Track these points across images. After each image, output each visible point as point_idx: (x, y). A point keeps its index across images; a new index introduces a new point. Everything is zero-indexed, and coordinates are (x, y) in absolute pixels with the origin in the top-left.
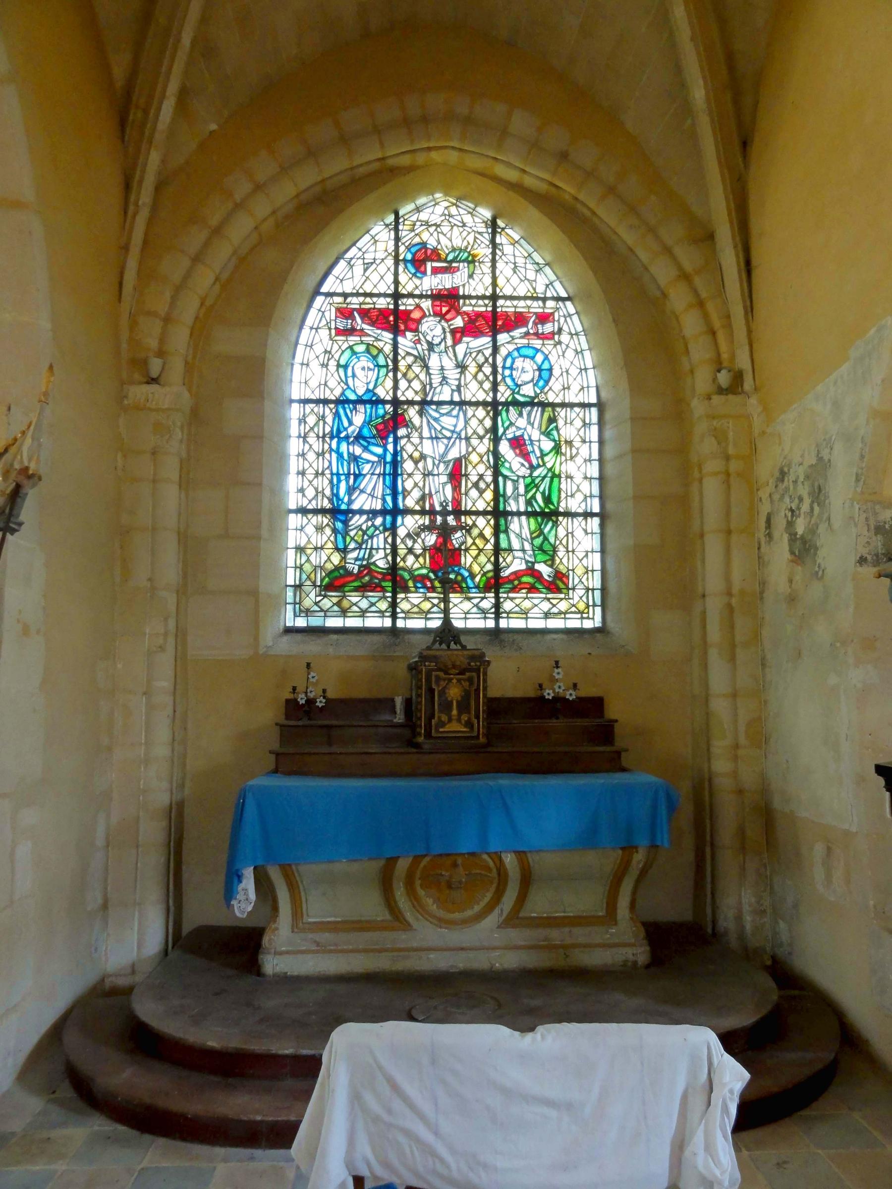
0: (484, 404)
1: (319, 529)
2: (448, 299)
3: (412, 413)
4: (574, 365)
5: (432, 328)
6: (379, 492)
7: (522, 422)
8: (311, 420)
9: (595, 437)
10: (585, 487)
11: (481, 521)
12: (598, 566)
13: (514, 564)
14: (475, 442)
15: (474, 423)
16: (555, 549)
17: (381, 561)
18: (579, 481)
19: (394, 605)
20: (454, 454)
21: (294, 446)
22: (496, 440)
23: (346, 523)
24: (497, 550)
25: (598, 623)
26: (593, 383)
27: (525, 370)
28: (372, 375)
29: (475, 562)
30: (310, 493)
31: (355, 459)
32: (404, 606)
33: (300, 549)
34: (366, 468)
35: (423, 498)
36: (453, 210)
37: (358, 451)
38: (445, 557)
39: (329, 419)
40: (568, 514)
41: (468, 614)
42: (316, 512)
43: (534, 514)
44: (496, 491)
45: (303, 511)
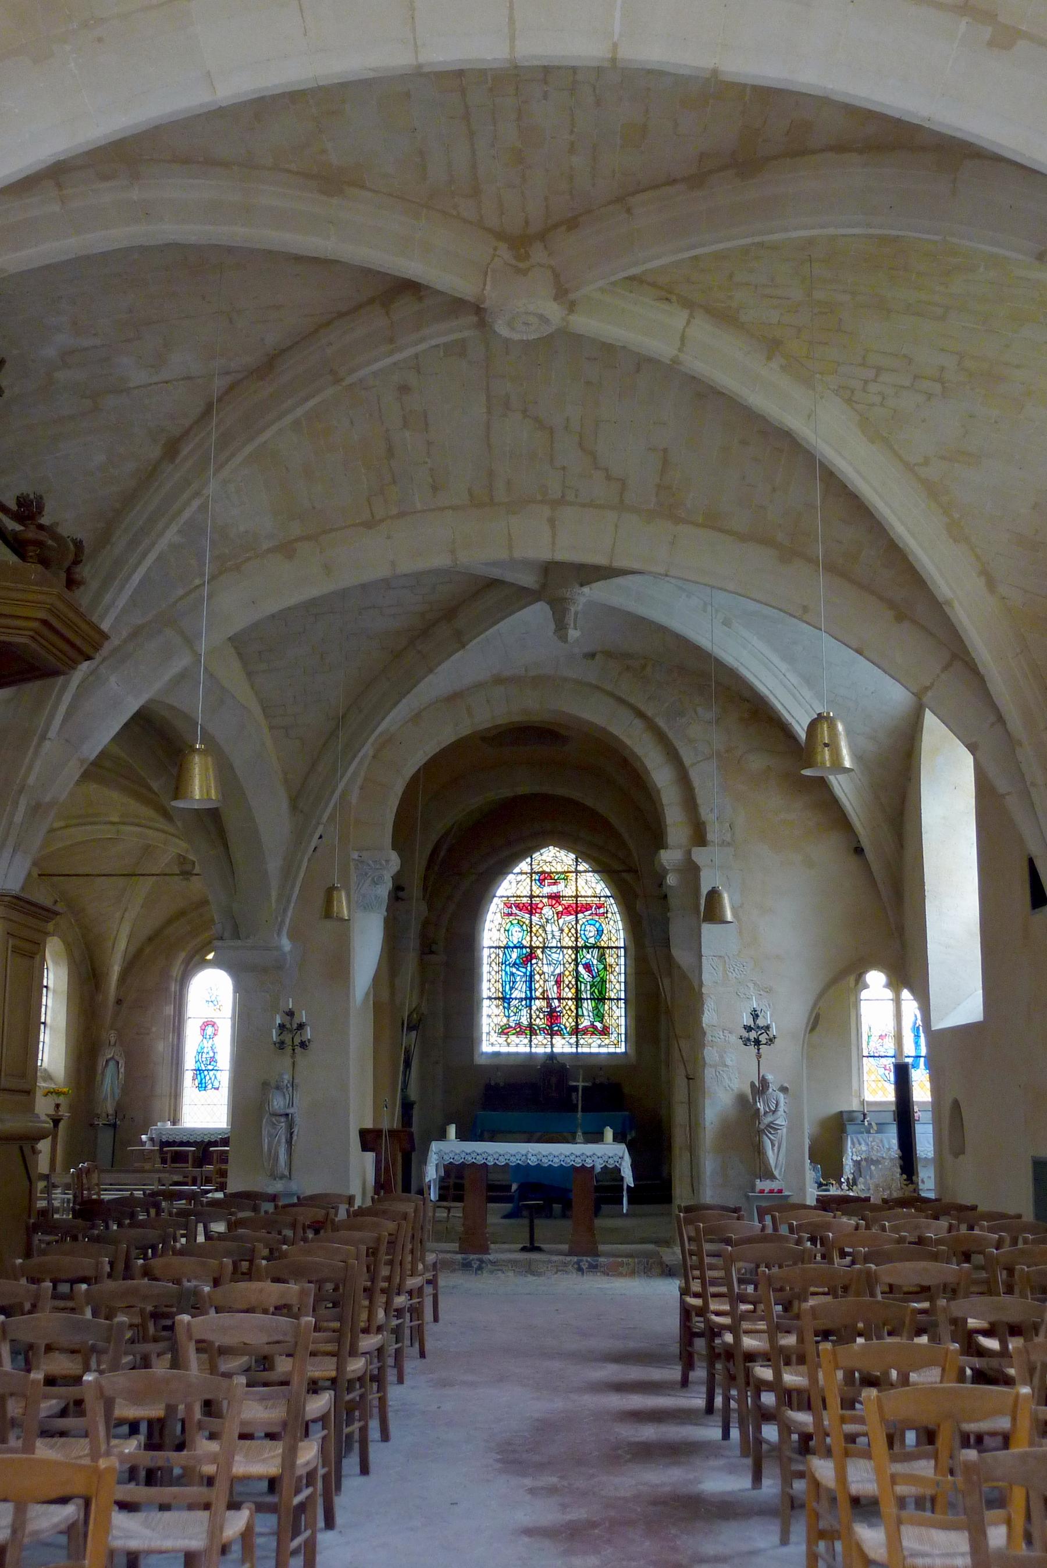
0: (572, 948)
1: (497, 1006)
2: (556, 897)
3: (539, 952)
4: (615, 930)
5: (548, 912)
6: (524, 990)
7: (589, 956)
8: (493, 956)
9: (623, 962)
10: (617, 986)
11: (570, 1003)
12: (623, 1023)
13: (585, 1023)
14: (567, 965)
15: (567, 956)
16: (603, 1016)
17: (525, 1021)
18: (617, 985)
19: (531, 1041)
20: (557, 971)
21: (485, 968)
22: (577, 965)
23: (509, 1004)
24: (577, 1016)
25: (623, 1050)
26: (622, 936)
27: (591, 931)
28: (521, 935)
29: (567, 1022)
30: (493, 990)
31: (513, 974)
32: (535, 1041)
33: (489, 1016)
34: (518, 978)
35: (544, 992)
36: (558, 854)
37: (514, 970)
38: (553, 1016)
39: (501, 955)
40: (610, 999)
41: (562, 1046)
42: (495, 999)
43: (594, 999)
44: (577, 988)
45: (490, 998)
